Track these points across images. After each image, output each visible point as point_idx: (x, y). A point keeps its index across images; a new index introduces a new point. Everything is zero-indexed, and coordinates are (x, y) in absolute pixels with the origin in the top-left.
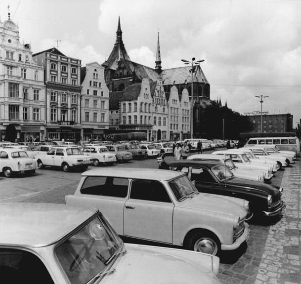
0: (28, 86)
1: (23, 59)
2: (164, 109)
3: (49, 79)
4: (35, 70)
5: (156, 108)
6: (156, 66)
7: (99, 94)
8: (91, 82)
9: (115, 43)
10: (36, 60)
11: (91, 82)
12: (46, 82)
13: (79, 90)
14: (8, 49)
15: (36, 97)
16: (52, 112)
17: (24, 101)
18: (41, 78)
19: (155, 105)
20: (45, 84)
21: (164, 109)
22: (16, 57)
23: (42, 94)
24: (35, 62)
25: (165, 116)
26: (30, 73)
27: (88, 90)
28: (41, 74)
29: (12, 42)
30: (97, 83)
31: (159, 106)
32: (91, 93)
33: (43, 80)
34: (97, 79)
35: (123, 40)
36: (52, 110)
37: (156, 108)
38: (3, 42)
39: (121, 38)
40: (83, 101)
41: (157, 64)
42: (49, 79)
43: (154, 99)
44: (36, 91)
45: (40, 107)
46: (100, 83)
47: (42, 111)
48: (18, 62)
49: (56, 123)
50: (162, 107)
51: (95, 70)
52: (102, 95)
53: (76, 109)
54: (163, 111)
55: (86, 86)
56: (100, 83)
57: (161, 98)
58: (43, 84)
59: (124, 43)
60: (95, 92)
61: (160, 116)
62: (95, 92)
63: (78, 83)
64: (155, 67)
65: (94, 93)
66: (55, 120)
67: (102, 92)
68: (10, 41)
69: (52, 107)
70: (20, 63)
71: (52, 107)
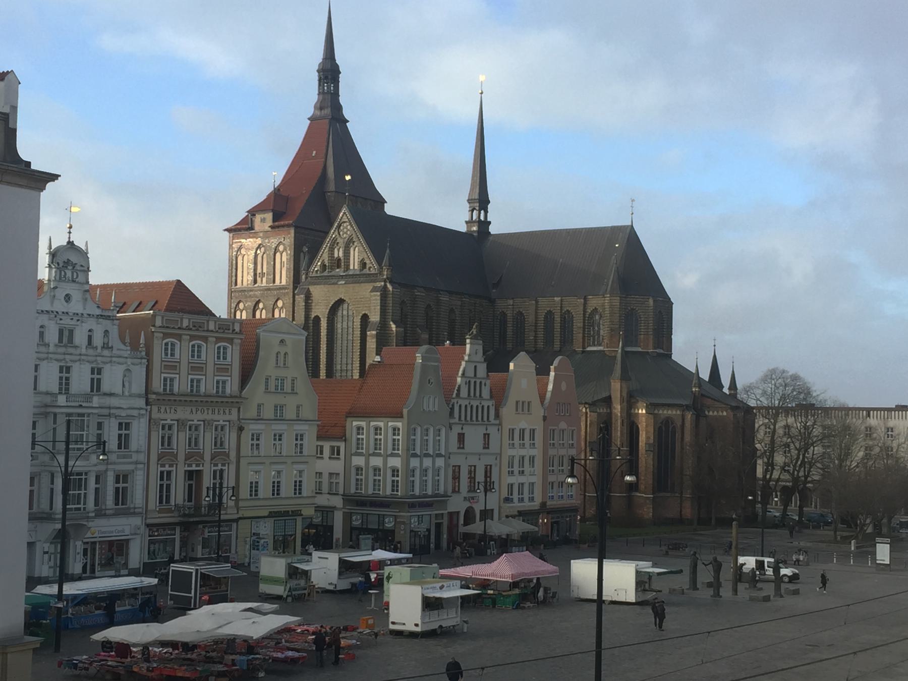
0: (106, 412)
1: (98, 340)
2: (487, 436)
4: (124, 367)
5: (461, 437)
6: (467, 220)
7: (290, 413)
9: (310, 111)
10: (128, 340)
13: (236, 401)
15: (124, 442)
16: (162, 479)
18: (138, 386)
19: (457, 429)
20: (147, 403)
21: (487, 436)
22: (80, 338)
23: (138, 432)
24: (124, 344)
25: (489, 460)
26: (112, 379)
28: (139, 372)
31: (469, 431)
32: (268, 413)
35: (342, 100)
36: (162, 473)
37: (461, 437)
38: (52, 303)
39: (336, 94)
40: (246, 437)
41: (472, 211)
42: (157, 385)
43: (452, 409)
44: (125, 426)
45: (131, 467)
47: (139, 479)
48: (84, 351)
49: (170, 511)
50: (481, 430)
51: (282, 341)
53: (223, 465)
54: (486, 446)
55: (256, 392)
57: (475, 403)
58: (141, 403)
59: (347, 113)
60: (279, 408)
61: (473, 460)
62: (279, 408)
63: (232, 386)
64: (467, 222)
65: (276, 410)
66: (168, 501)
67: (298, 407)
68: (68, 298)
69: (163, 466)
70: (91, 352)
71: (163, 466)
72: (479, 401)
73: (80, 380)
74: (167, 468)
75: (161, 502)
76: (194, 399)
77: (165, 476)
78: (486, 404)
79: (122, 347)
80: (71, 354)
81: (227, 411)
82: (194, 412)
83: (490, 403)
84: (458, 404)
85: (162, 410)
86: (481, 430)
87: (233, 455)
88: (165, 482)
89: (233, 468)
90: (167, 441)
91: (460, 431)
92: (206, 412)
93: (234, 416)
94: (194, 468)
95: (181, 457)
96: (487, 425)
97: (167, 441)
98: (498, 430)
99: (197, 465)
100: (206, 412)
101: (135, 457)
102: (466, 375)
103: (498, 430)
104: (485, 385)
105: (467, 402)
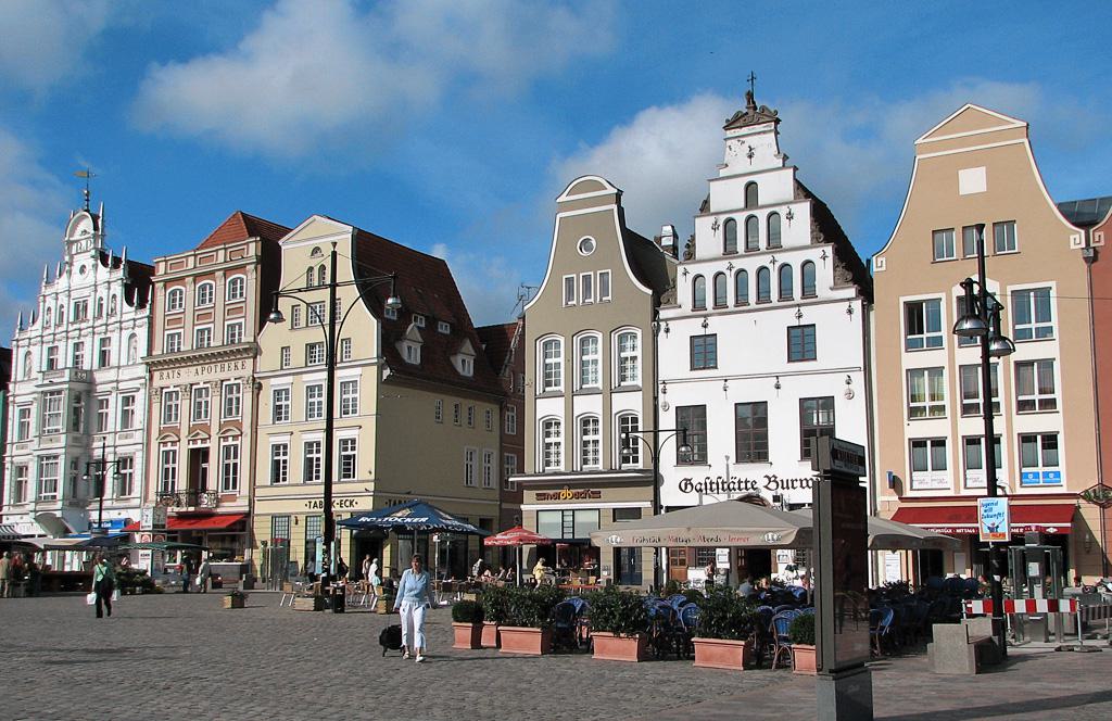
57: (751, 265)
72: (769, 257)
76: (203, 357)
77: (169, 457)
78: (795, 258)
80: (80, 330)
81: (240, 365)
82: (200, 373)
83: (814, 254)
84: (690, 277)
85: (165, 376)
86: (788, 317)
90: (170, 413)
91: (702, 332)
92: (213, 370)
93: (248, 372)
94: (199, 445)
96: (799, 305)
97: (170, 413)
98: (850, 312)
99: (203, 440)
100: (213, 370)
102: (713, 209)
103: (850, 312)
104: (790, 216)
105: (722, 266)
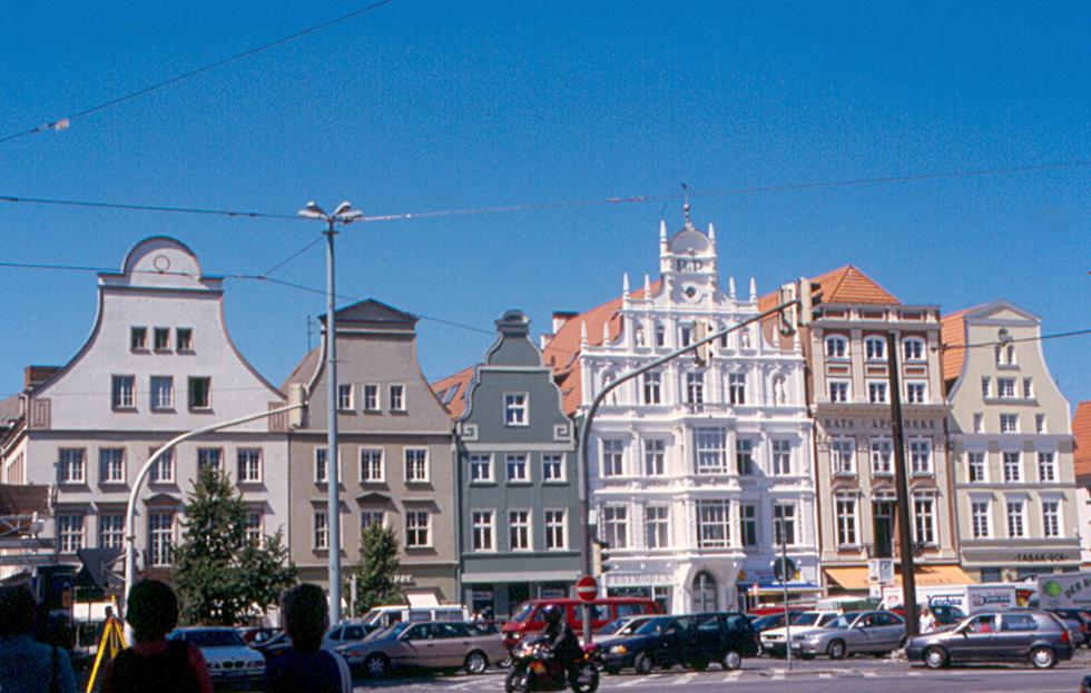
3: (822, 396)
8: (985, 383)
11: (985, 383)
12: (814, 407)
14: (682, 320)
16: (840, 511)
17: (741, 483)
20: (810, 415)
27: (978, 417)
29: (697, 296)
30: (1011, 383)
33: (801, 403)
34: (1009, 367)
36: (840, 506)
46: (1027, 383)
51: (1002, 332)
52: (1039, 429)
56: (1027, 383)
58: (801, 418)
66: (852, 539)
73: (714, 387)
74: (845, 499)
75: (842, 540)
79: (767, 347)
87: (942, 483)
88: (845, 515)
89: (944, 501)
95: (865, 485)
101: (803, 487)
